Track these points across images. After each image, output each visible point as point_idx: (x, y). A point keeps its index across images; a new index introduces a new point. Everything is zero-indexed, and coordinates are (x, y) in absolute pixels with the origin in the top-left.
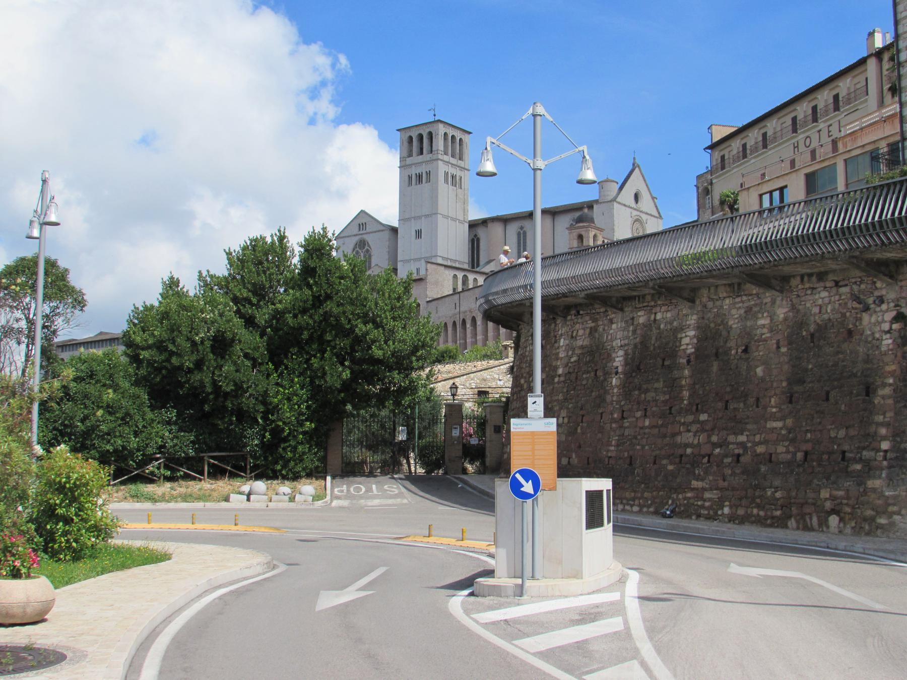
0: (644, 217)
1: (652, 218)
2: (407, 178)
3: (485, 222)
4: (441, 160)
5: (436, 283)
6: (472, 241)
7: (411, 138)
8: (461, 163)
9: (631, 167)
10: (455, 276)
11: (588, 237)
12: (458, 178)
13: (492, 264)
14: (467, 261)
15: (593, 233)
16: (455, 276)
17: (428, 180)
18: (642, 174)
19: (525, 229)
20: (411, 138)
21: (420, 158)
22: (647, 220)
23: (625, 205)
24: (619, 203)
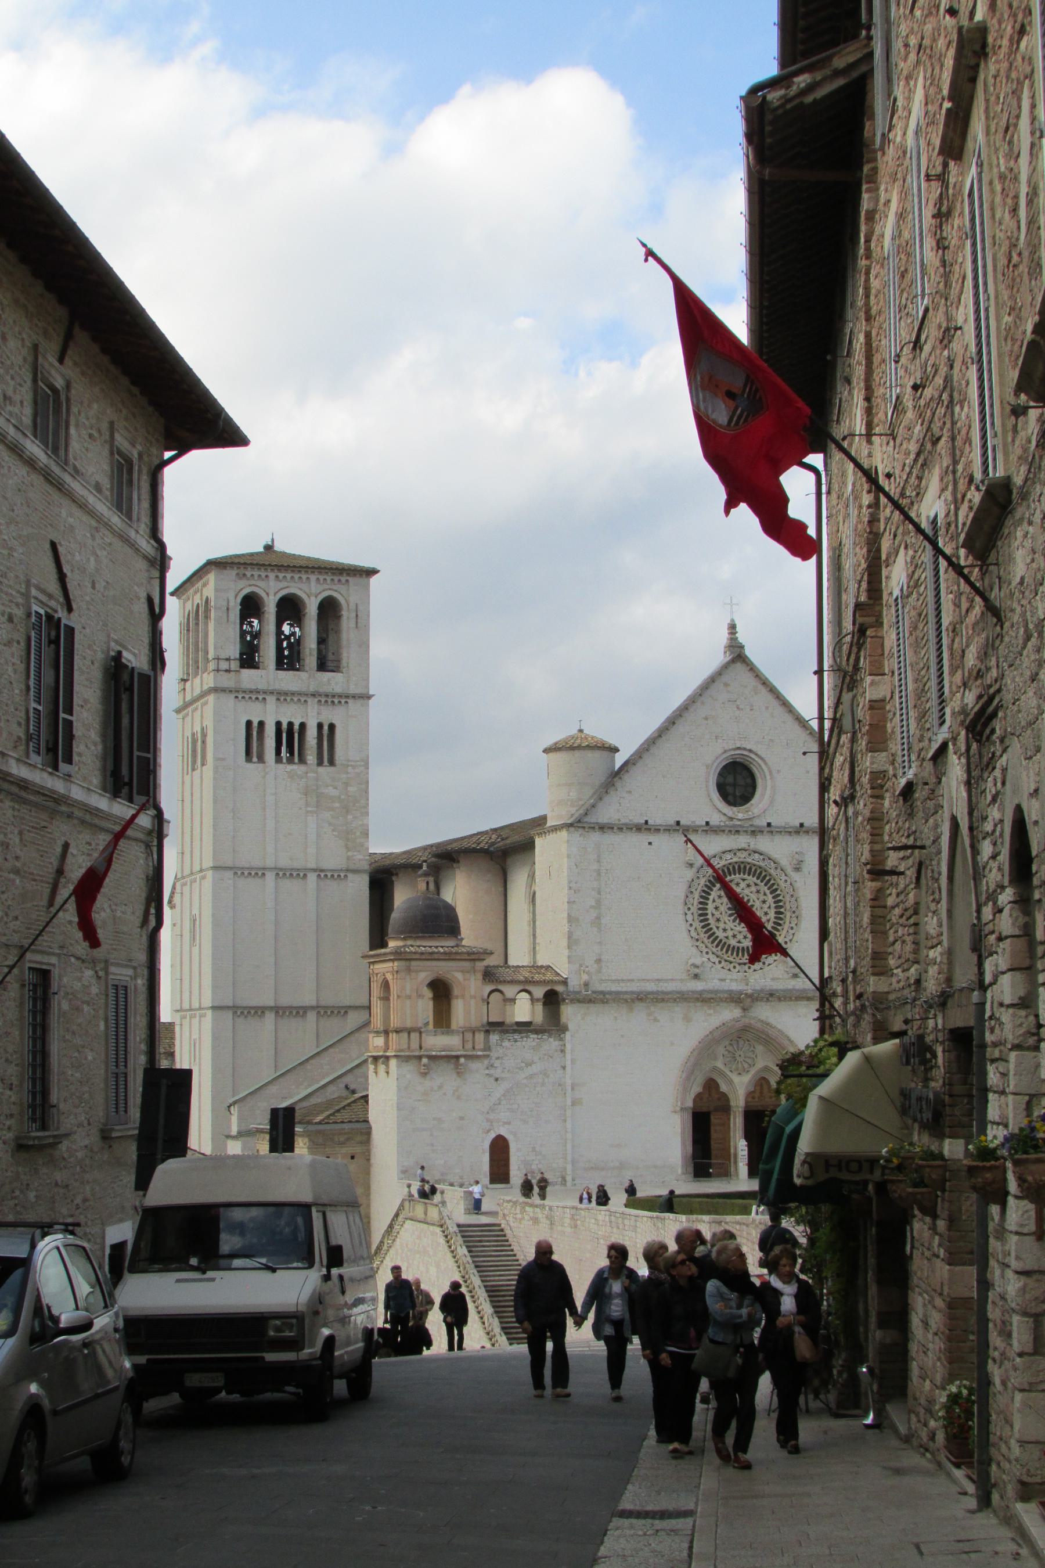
9: (718, 657)
12: (312, 733)
15: (424, 976)
23: (644, 828)
24: (602, 828)
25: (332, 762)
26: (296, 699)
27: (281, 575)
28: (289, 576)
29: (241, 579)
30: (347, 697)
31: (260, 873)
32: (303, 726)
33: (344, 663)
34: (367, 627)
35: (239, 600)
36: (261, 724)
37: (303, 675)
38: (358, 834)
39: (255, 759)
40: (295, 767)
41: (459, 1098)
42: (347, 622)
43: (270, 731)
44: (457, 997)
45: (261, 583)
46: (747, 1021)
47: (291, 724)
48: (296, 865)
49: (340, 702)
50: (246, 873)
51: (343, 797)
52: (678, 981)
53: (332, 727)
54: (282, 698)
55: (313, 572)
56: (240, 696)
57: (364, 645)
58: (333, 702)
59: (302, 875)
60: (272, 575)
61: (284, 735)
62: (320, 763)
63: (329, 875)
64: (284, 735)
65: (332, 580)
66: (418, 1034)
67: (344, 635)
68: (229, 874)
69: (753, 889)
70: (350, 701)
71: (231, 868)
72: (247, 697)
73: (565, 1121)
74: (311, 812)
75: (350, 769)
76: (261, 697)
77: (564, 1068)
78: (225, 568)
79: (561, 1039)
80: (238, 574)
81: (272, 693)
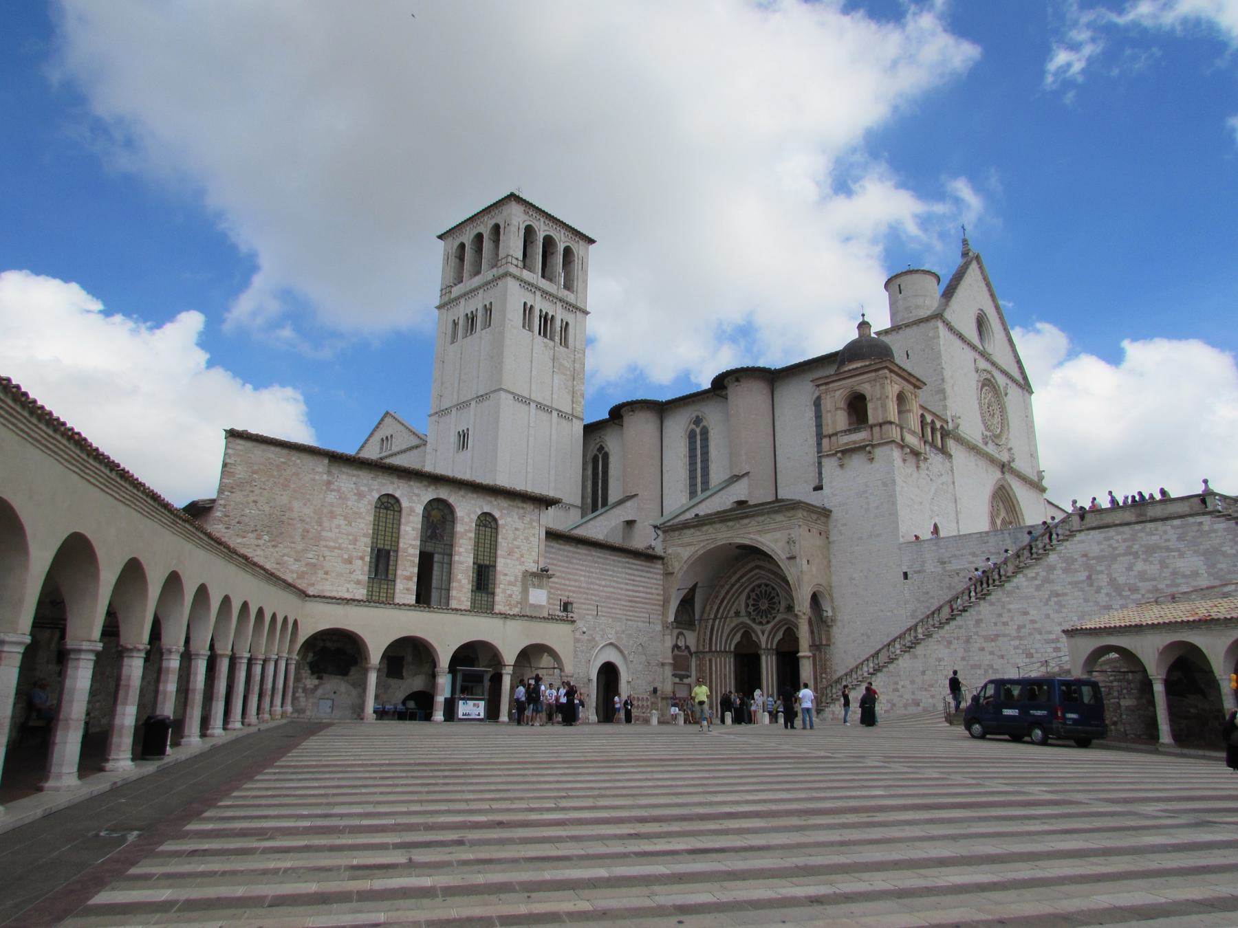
0: (1001, 380)
1: (1014, 385)
2: (450, 325)
3: (617, 414)
4: (514, 277)
5: (277, 527)
6: (595, 460)
7: (462, 246)
8: (571, 297)
10: (388, 505)
11: (883, 399)
12: (558, 324)
13: (629, 504)
14: (579, 503)
16: (388, 505)
17: (488, 323)
18: (985, 278)
19: (704, 423)
20: (462, 246)
21: (477, 281)
22: (1006, 388)
24: (951, 329)
25: (566, 346)
27: (547, 222)
29: (525, 214)
34: (586, 272)
37: (555, 287)
40: (548, 341)
41: (918, 487)
43: (537, 313)
44: (909, 411)
45: (535, 221)
46: (1002, 482)
47: (547, 313)
48: (545, 403)
52: (980, 444)
57: (585, 282)
60: (542, 220)
62: (561, 344)
66: (898, 429)
69: (993, 400)
70: (578, 312)
71: (512, 393)
72: (526, 287)
73: (958, 523)
77: (954, 483)
79: (951, 462)
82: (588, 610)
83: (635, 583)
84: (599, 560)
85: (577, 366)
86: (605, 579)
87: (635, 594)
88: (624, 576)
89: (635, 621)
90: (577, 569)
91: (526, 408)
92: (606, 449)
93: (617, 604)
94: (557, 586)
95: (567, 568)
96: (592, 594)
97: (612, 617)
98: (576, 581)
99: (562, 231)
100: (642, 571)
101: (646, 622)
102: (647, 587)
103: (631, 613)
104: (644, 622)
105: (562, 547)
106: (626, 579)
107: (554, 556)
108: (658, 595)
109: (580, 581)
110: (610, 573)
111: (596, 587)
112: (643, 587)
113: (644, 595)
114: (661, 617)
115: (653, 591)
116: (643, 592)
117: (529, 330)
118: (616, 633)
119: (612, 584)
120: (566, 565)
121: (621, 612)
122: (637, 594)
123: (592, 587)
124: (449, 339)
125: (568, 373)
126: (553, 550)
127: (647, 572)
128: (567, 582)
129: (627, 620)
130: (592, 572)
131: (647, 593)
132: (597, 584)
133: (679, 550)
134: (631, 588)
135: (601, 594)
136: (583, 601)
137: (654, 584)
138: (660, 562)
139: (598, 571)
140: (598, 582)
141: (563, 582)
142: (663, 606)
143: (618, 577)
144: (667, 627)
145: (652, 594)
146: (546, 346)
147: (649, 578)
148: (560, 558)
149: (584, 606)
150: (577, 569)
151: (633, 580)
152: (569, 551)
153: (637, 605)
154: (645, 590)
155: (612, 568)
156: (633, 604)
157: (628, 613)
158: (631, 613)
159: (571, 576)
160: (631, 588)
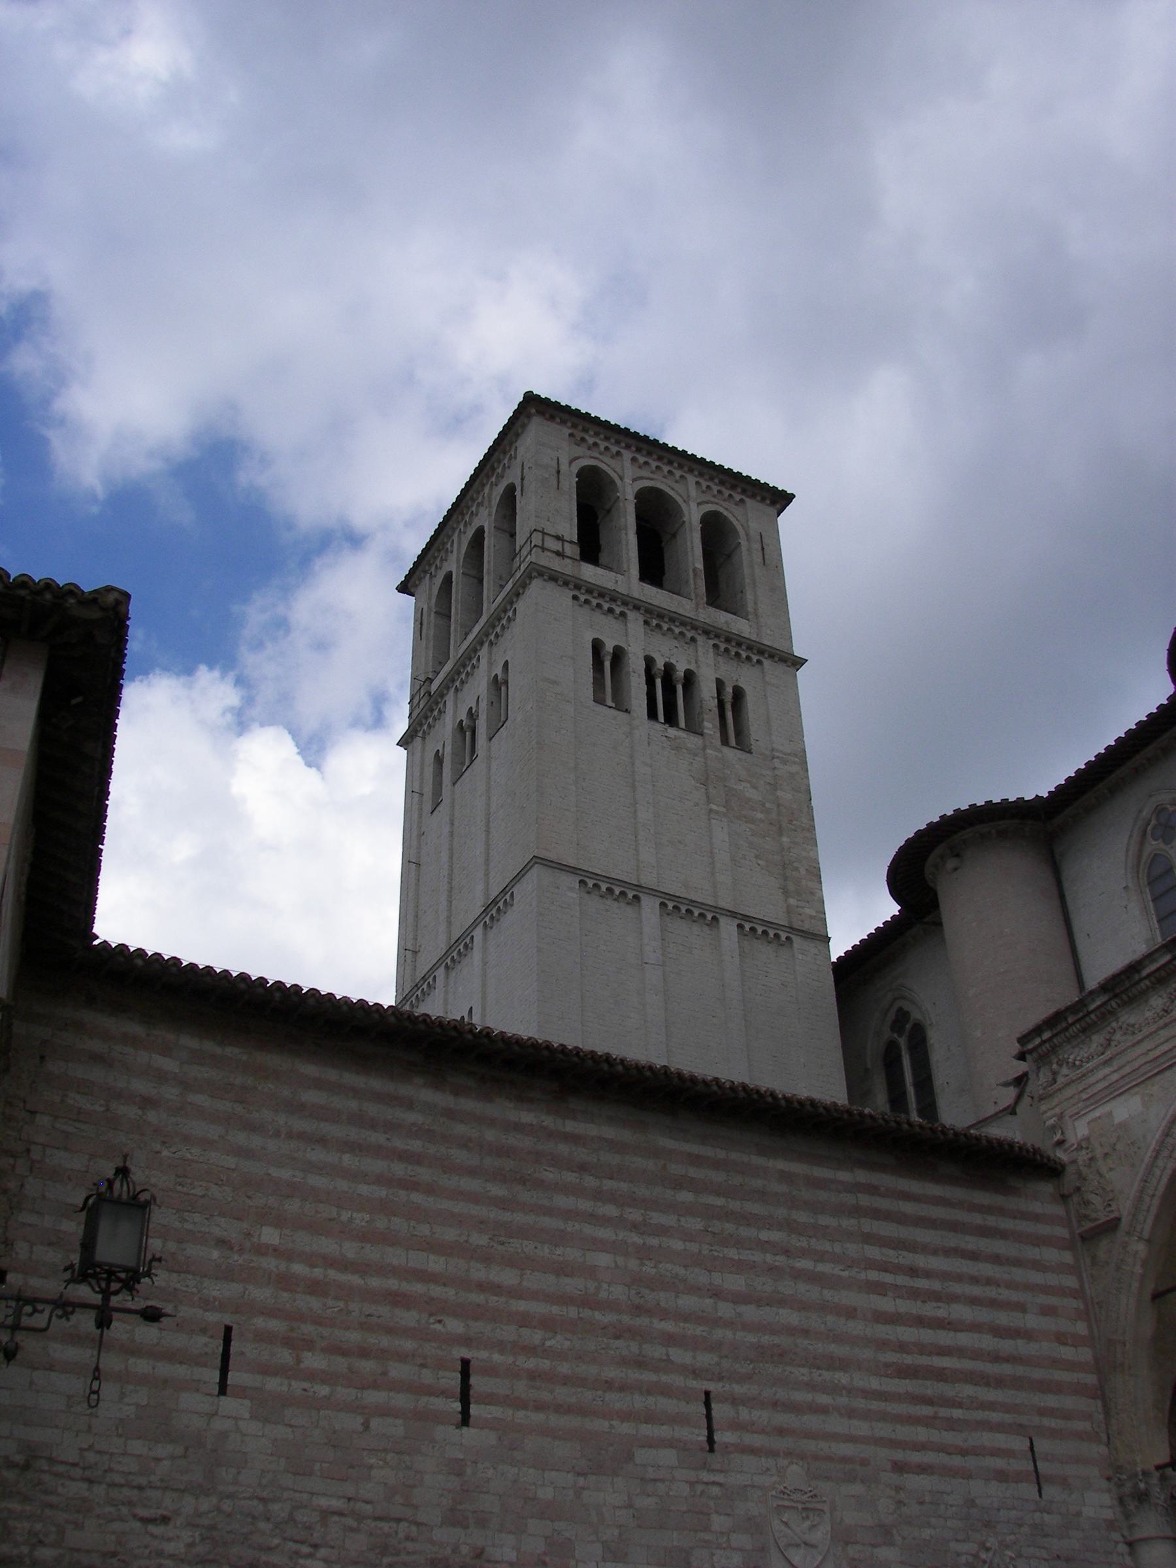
4: (553, 577)
12: (707, 691)
25: (742, 744)
26: (677, 631)
27: (642, 459)
28: (654, 464)
30: (761, 652)
31: (630, 895)
32: (689, 678)
33: (750, 609)
35: (575, 469)
36: (618, 655)
38: (803, 871)
39: (610, 703)
42: (747, 556)
47: (669, 669)
49: (748, 658)
50: (604, 887)
51: (768, 805)
53: (738, 694)
54: (654, 622)
55: (691, 471)
56: (582, 598)
58: (738, 655)
59: (709, 916)
60: (627, 455)
61: (659, 682)
62: (725, 741)
63: (760, 930)
64: (659, 682)
65: (719, 492)
67: (746, 571)
68: (573, 881)
70: (767, 663)
71: (574, 870)
72: (594, 602)
74: (717, 812)
75: (777, 763)
76: (618, 610)
78: (552, 418)
80: (571, 435)
81: (637, 608)
82: (650, 1418)
83: (922, 1283)
84: (693, 1172)
85: (785, 795)
86: (739, 1266)
87: (928, 1336)
88: (852, 1249)
89: (953, 1472)
90: (569, 1215)
91: (629, 910)
92: (916, 1015)
93: (836, 1389)
94: (437, 1291)
95: (501, 1204)
96: (670, 1340)
97: (789, 1454)
98: (562, 1270)
99: (691, 479)
100: (955, 1227)
101: (1019, 1478)
102: (993, 1304)
103: (921, 1434)
104: (1002, 1476)
105: (468, 1104)
106: (871, 1264)
107: (416, 1145)
108: (1061, 1338)
109: (591, 1272)
110: (775, 1236)
111: (687, 1302)
112: (974, 1301)
113: (988, 1342)
114: (1098, 1450)
115: (1032, 1321)
116: (975, 1327)
117: (617, 708)
118: (843, 1537)
119: (787, 1287)
120: (497, 1190)
121: (861, 1428)
122: (945, 1338)
123: (664, 1299)
124: (428, 807)
125: (760, 816)
126: (412, 1117)
127: (984, 1232)
128: (508, 1277)
129: (899, 1467)
130: (662, 1231)
131: (998, 1332)
132: (695, 1290)
133: (1124, 1109)
134: (905, 1306)
135: (719, 1334)
136: (612, 1373)
137: (1029, 1287)
138: (1047, 1188)
139: (695, 1224)
140: (700, 1277)
141: (479, 1272)
142: (1100, 1393)
143: (821, 1257)
144: (1142, 1497)
145: (1027, 1335)
146: (677, 748)
147: (996, 1259)
148: (459, 1156)
149: (616, 1401)
150: (569, 1215)
151: (913, 1272)
152: (518, 1127)
153: (947, 1390)
154: (983, 1315)
155: (781, 1212)
156: (930, 1388)
157: (904, 1432)
158: (921, 1434)
159: (528, 1246)
160: (905, 1306)
